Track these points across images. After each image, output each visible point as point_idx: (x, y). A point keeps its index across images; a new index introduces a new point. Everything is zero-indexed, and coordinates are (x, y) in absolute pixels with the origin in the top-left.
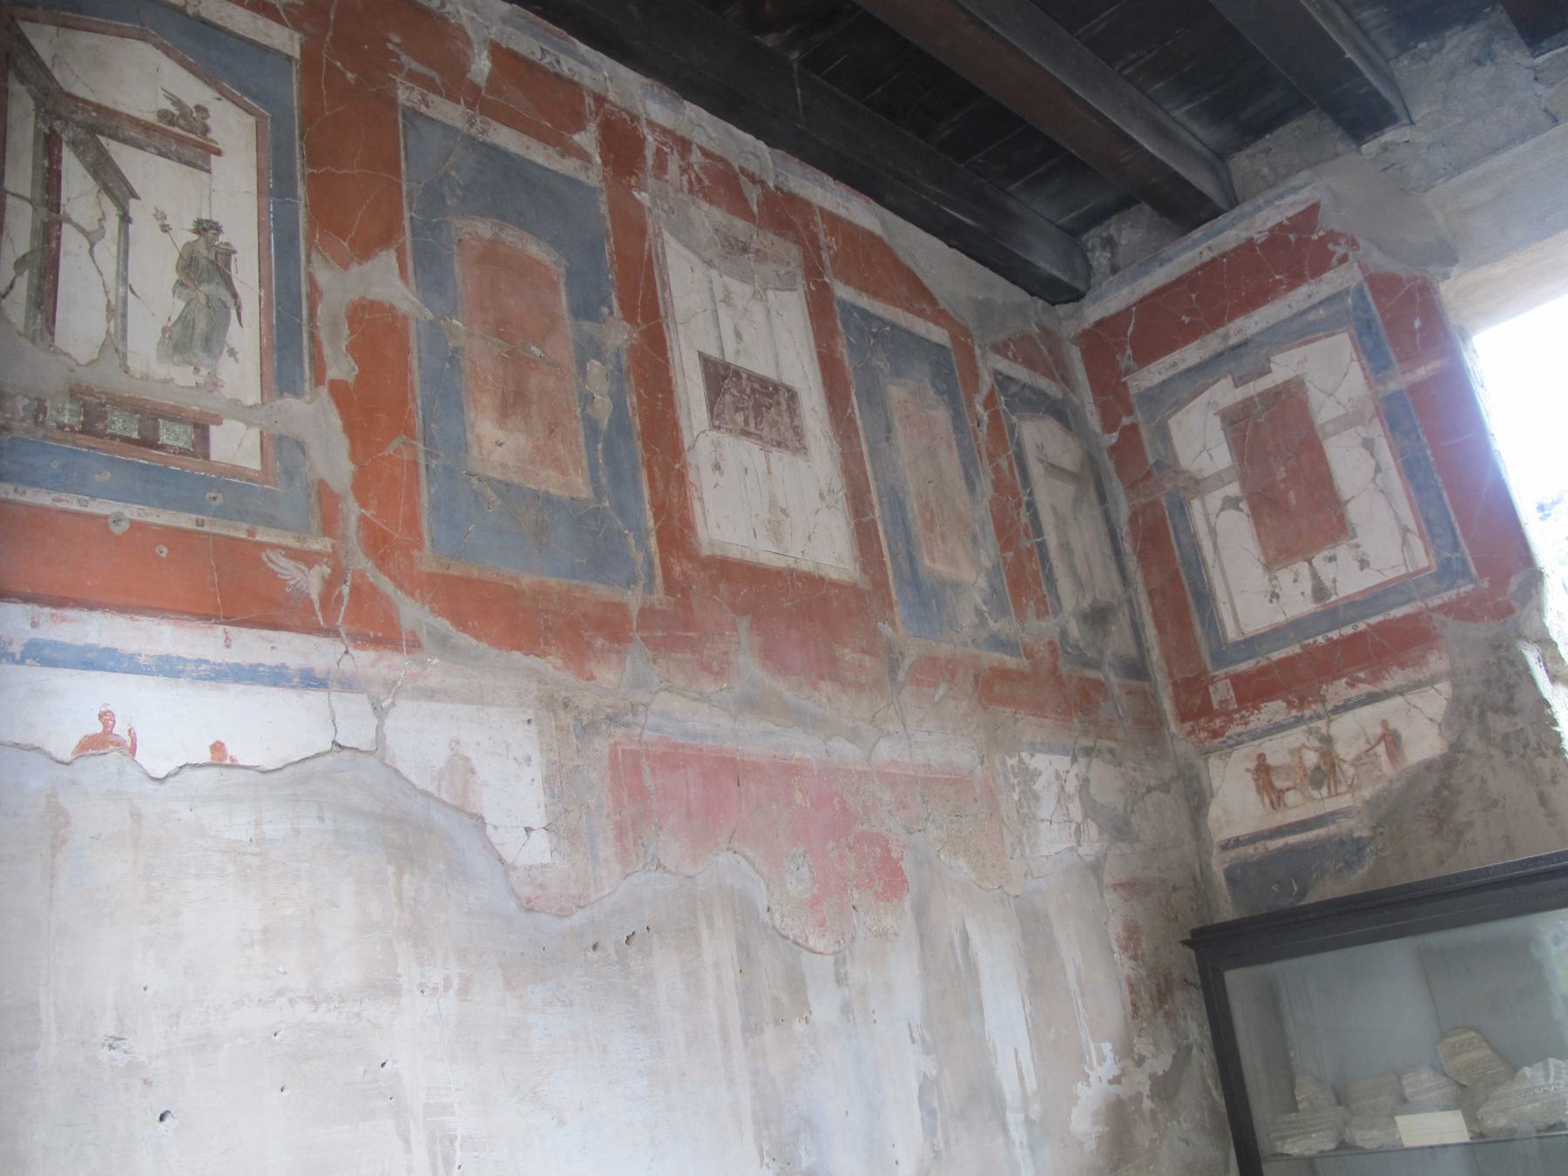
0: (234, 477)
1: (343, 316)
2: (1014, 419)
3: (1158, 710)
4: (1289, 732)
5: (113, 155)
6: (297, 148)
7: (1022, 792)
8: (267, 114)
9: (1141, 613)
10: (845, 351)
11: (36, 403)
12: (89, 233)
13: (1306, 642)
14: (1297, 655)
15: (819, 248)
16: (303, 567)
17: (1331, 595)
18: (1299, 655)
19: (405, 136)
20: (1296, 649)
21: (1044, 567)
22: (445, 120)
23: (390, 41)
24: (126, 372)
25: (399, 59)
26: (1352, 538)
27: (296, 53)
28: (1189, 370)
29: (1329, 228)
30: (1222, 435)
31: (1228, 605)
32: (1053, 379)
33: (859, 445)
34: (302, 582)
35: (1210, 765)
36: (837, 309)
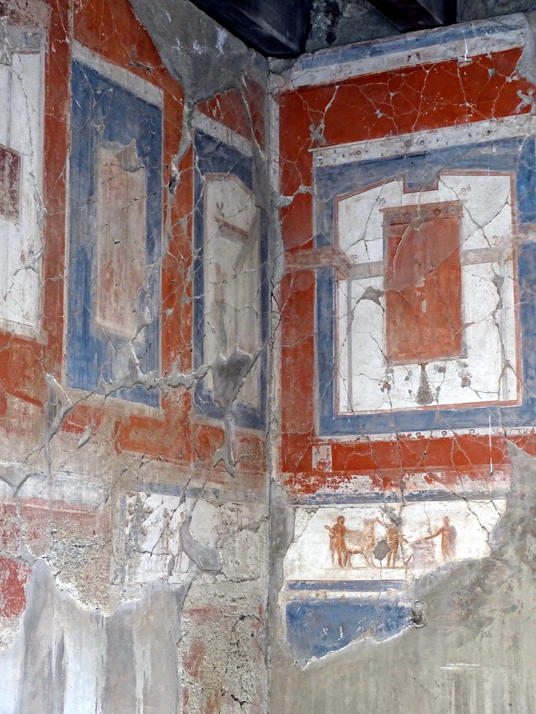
2: (203, 178)
3: (265, 456)
4: (368, 505)
7: (133, 527)
9: (271, 364)
10: (69, 115)
13: (402, 433)
14: (391, 441)
15: (67, 7)
17: (432, 400)
18: (394, 443)
20: (393, 438)
21: (196, 323)
26: (463, 358)
28: (369, 162)
29: (523, 76)
30: (380, 232)
31: (346, 382)
32: (248, 136)
33: (64, 209)
35: (297, 515)
36: (71, 72)
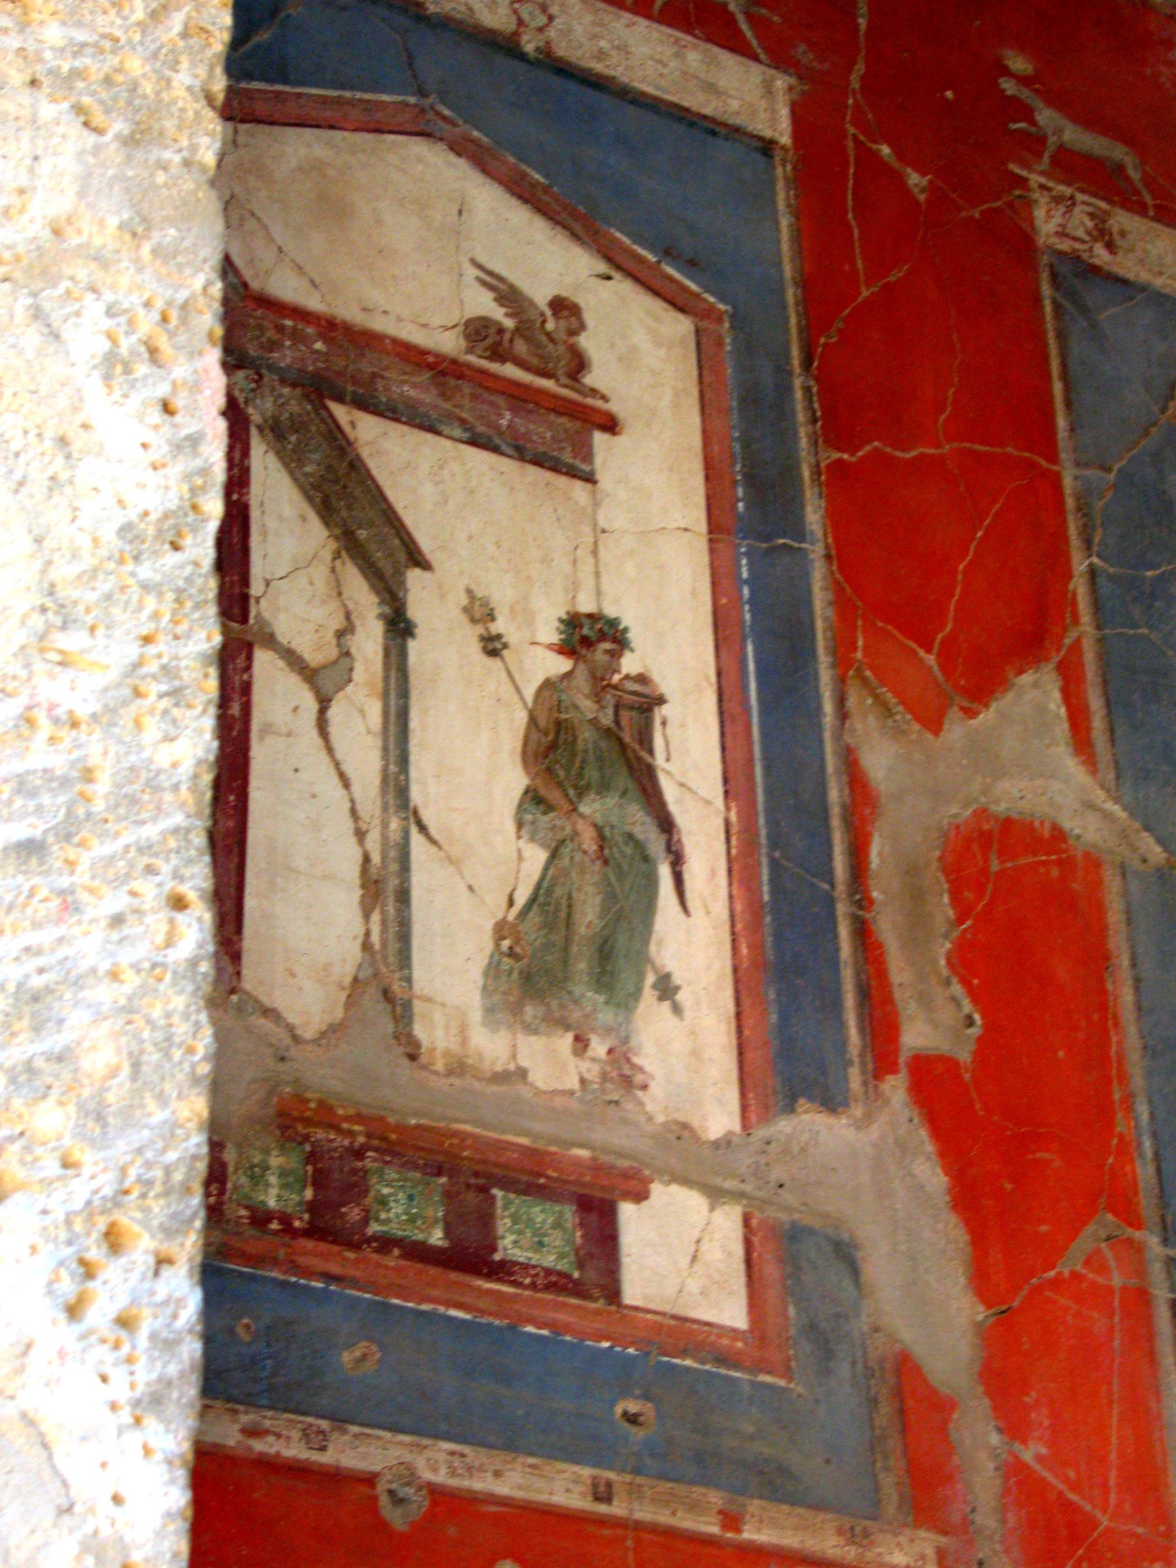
0: (684, 1353)
1: (934, 865)
5: (365, 453)
6: (798, 394)
8: (721, 307)
19: (1061, 336)
22: (1159, 282)
23: (1006, 72)
24: (413, 1057)
25: (1033, 122)
27: (782, 130)
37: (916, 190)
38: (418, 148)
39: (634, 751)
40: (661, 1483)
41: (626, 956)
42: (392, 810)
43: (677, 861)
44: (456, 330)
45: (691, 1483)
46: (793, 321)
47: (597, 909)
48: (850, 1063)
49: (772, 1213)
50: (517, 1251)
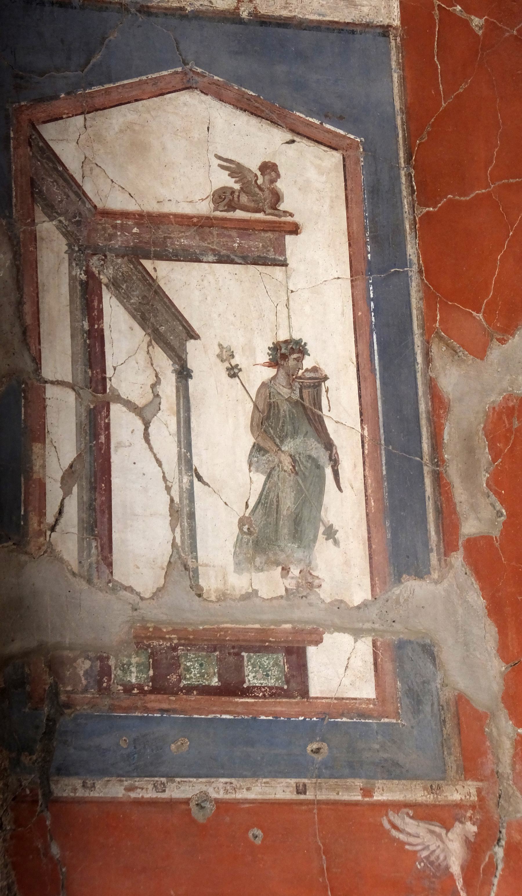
0: (342, 715)
6: (403, 180)
11: (98, 663)
12: (142, 409)
16: (437, 829)
24: (200, 596)
34: (438, 852)
37: (477, 29)
38: (185, 97)
39: (311, 410)
40: (331, 780)
41: (308, 521)
42: (183, 472)
43: (335, 462)
44: (209, 199)
45: (347, 777)
46: (400, 136)
47: (293, 499)
48: (432, 551)
49: (388, 637)
50: (255, 681)
